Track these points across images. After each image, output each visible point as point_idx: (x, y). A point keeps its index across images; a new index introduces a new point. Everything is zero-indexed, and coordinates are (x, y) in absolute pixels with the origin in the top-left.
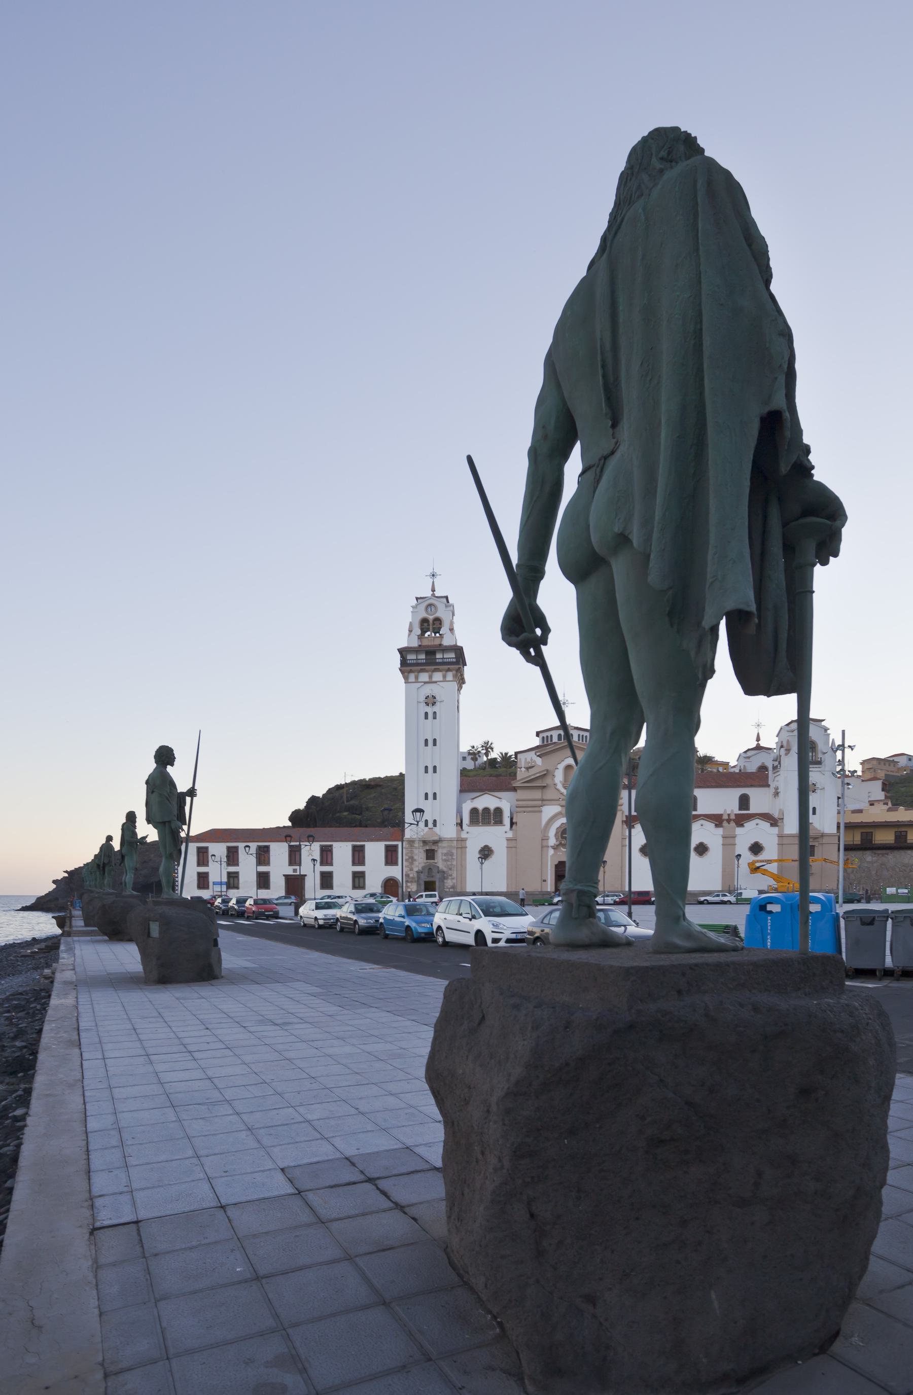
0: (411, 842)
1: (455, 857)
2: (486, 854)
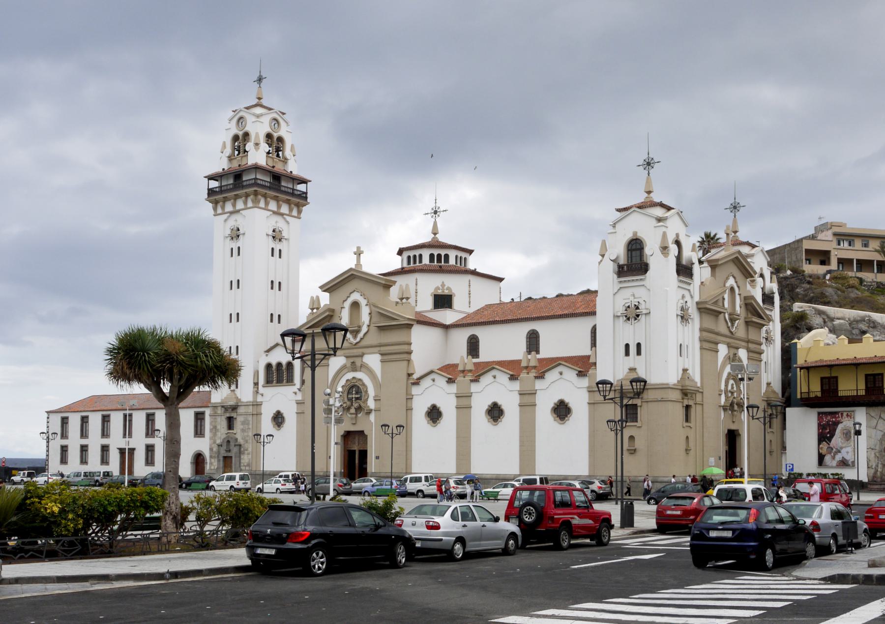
0: (215, 407)
1: (251, 427)
2: (280, 423)
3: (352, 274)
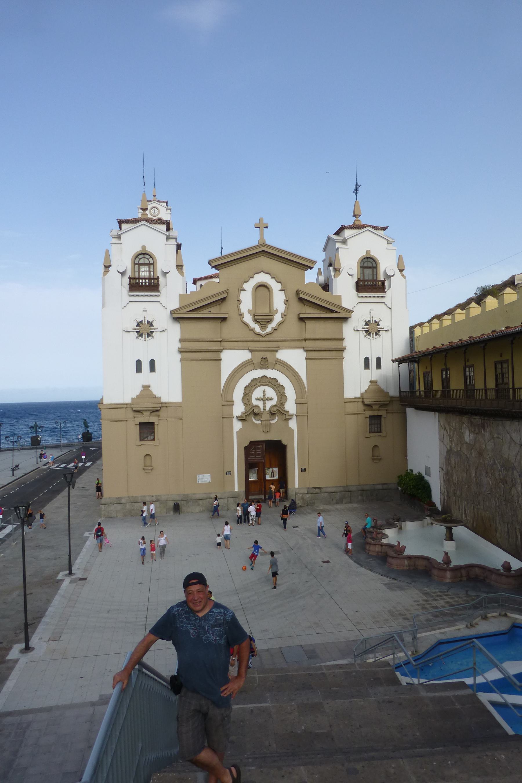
3: (263, 251)
